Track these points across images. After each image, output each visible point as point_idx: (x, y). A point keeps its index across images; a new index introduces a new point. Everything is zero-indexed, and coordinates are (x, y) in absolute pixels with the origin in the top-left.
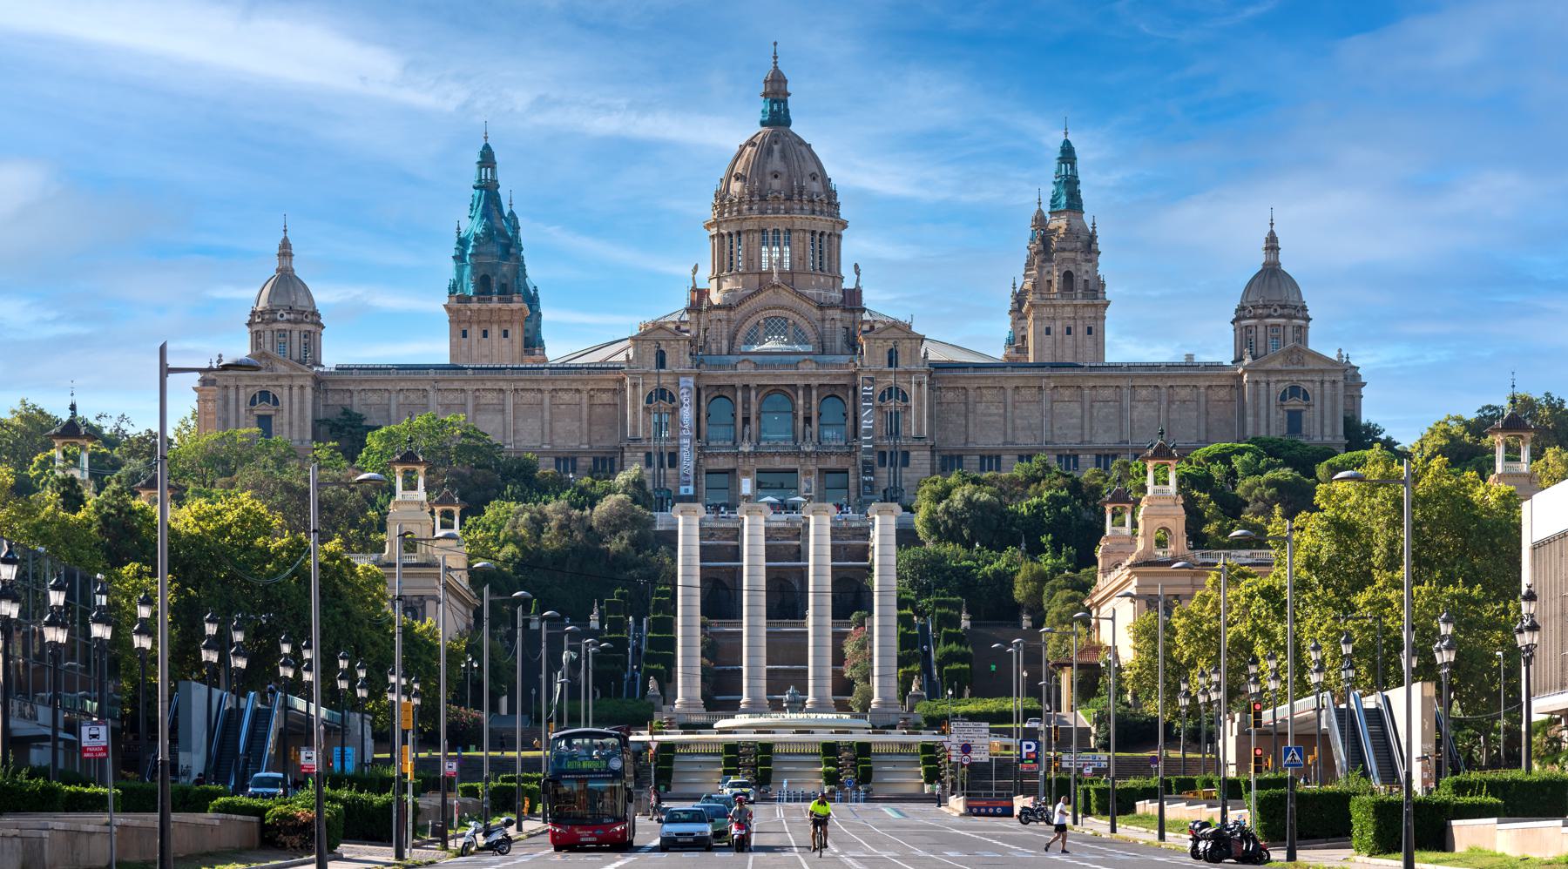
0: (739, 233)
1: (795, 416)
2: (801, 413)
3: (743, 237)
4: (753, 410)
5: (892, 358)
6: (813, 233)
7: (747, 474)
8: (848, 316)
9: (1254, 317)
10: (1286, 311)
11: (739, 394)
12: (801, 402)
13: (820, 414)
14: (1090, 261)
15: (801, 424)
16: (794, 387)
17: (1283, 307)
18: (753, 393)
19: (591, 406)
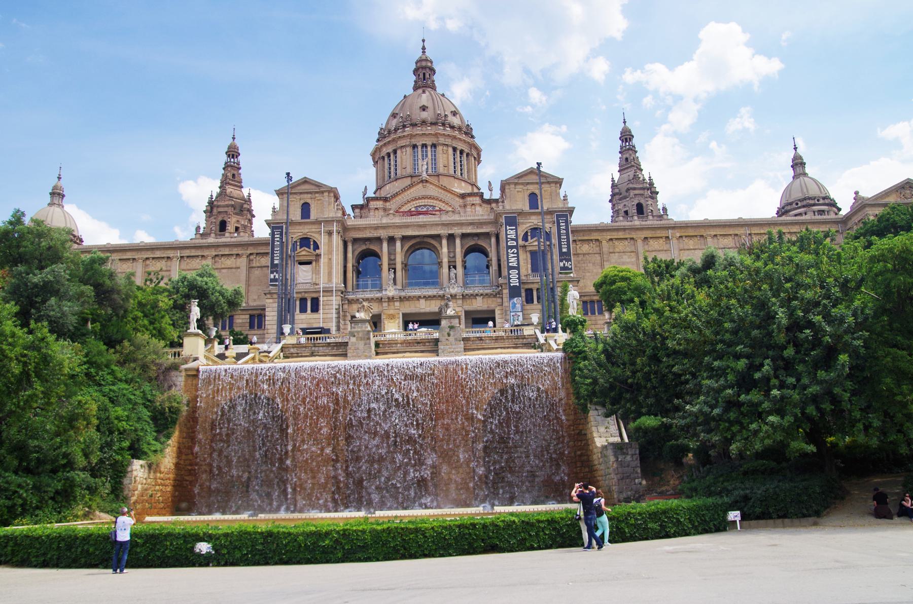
0: (395, 152)
1: (440, 264)
2: (445, 260)
3: (399, 152)
4: (399, 259)
5: (533, 199)
6: (455, 149)
7: (392, 317)
8: (484, 205)
9: (804, 206)
10: (827, 201)
11: (385, 245)
12: (445, 250)
13: (465, 268)
14: (652, 198)
15: (445, 270)
16: (438, 237)
17: (824, 198)
18: (398, 244)
19: (250, 268)
